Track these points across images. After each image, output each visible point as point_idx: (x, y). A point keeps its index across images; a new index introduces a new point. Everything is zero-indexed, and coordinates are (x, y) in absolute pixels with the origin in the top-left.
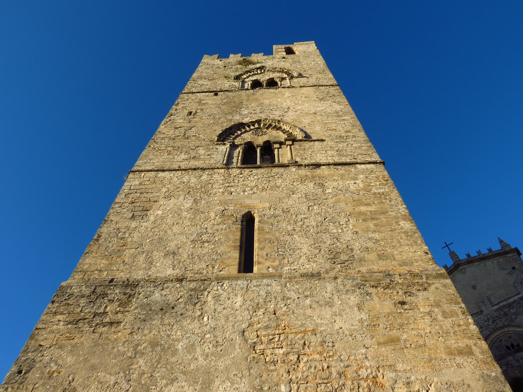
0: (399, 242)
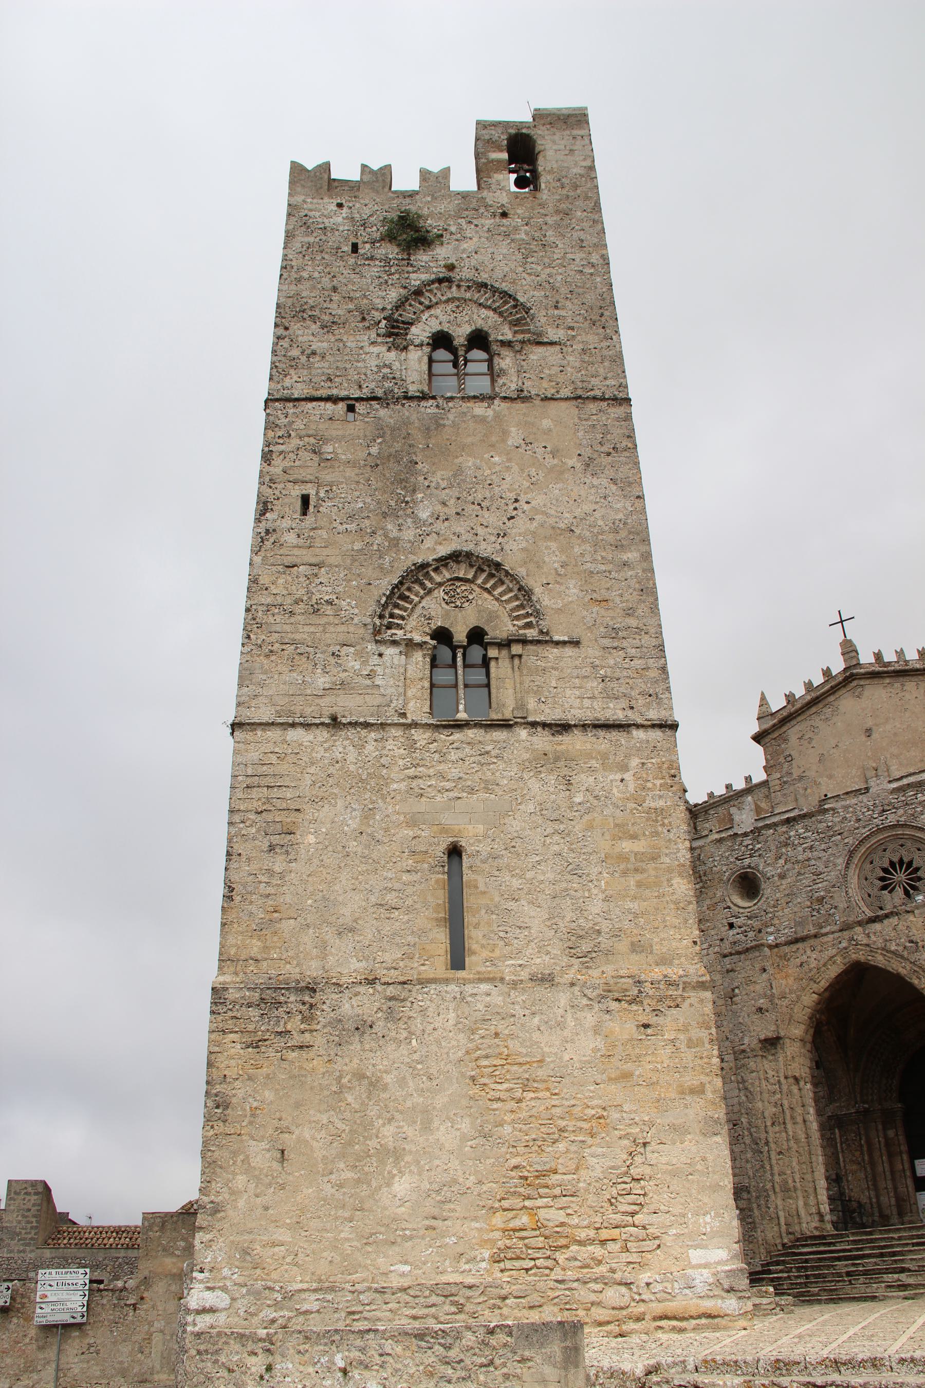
0: (664, 921)
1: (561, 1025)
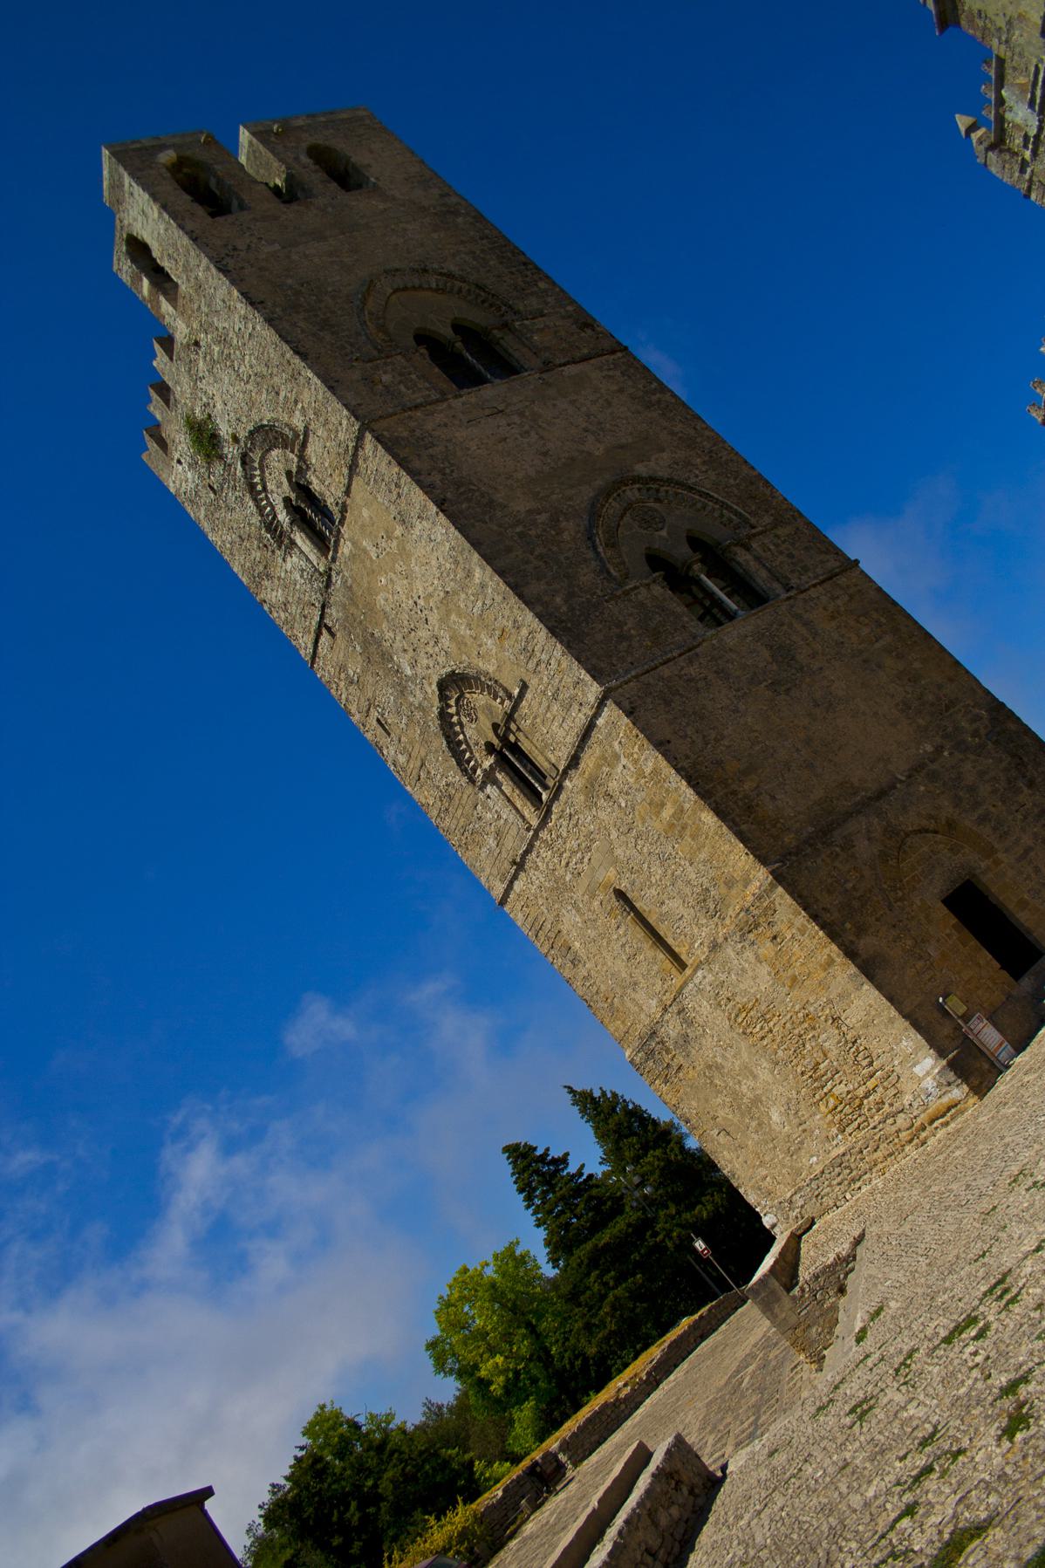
1: (743, 970)
